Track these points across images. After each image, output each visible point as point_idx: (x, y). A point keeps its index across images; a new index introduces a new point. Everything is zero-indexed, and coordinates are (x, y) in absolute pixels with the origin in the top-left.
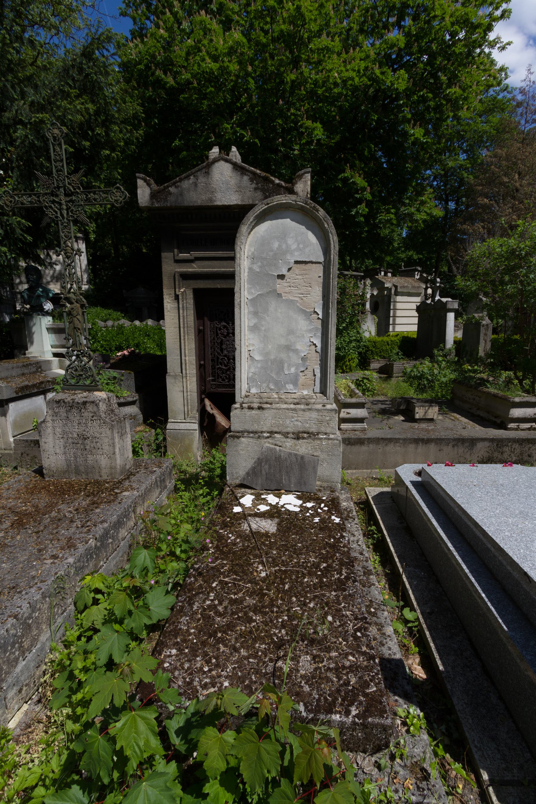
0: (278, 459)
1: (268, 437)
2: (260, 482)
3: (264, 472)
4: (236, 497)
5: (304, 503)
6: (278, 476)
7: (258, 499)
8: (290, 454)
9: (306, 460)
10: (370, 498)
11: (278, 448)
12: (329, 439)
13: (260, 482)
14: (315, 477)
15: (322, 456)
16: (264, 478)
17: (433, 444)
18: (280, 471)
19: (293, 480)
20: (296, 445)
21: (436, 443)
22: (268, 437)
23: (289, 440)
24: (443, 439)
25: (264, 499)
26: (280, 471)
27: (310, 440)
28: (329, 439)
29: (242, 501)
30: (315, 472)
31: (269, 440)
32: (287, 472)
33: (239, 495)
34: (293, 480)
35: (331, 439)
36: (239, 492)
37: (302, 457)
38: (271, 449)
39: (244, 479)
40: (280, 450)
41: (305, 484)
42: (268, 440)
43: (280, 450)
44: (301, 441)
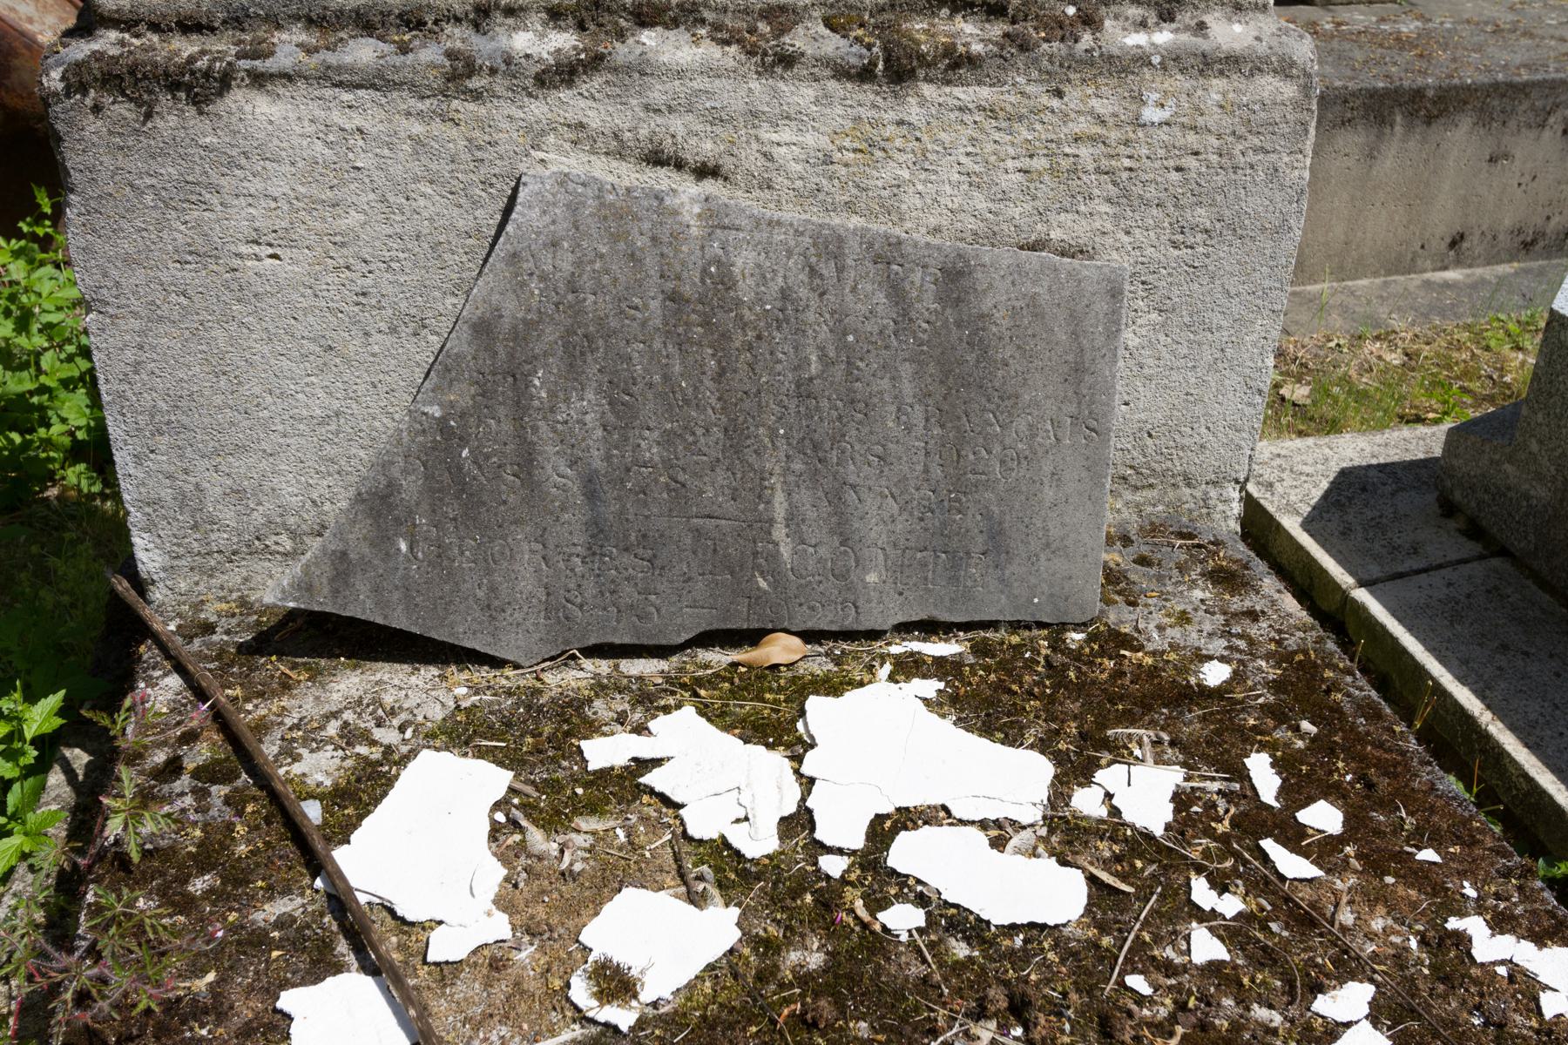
0: (704, 309)
1: (564, 73)
2: (525, 575)
3: (556, 471)
4: (280, 808)
5: (1075, 771)
6: (713, 489)
7: (566, 806)
8: (830, 246)
9: (996, 298)
10: (1292, 524)
11: (688, 193)
12: (1210, 64)
13: (525, 575)
14: (1094, 467)
15: (1123, 246)
16: (572, 527)
17: (1466, 122)
18: (736, 436)
19: (879, 520)
20: (871, 148)
21: (1485, 118)
22: (564, 73)
23: (800, 93)
24: (1522, 90)
25: (627, 784)
26: (736, 436)
27: (1022, 88)
28: (1210, 64)
29: (370, 861)
30: (1092, 424)
31: (580, 103)
32: (811, 446)
33: (319, 767)
34: (879, 520)
35: (1231, 63)
36: (312, 720)
37: (955, 278)
38: (617, 213)
39: (342, 566)
40: (716, 219)
41: (997, 542)
42: (572, 103)
43: (716, 219)
44: (928, 98)
